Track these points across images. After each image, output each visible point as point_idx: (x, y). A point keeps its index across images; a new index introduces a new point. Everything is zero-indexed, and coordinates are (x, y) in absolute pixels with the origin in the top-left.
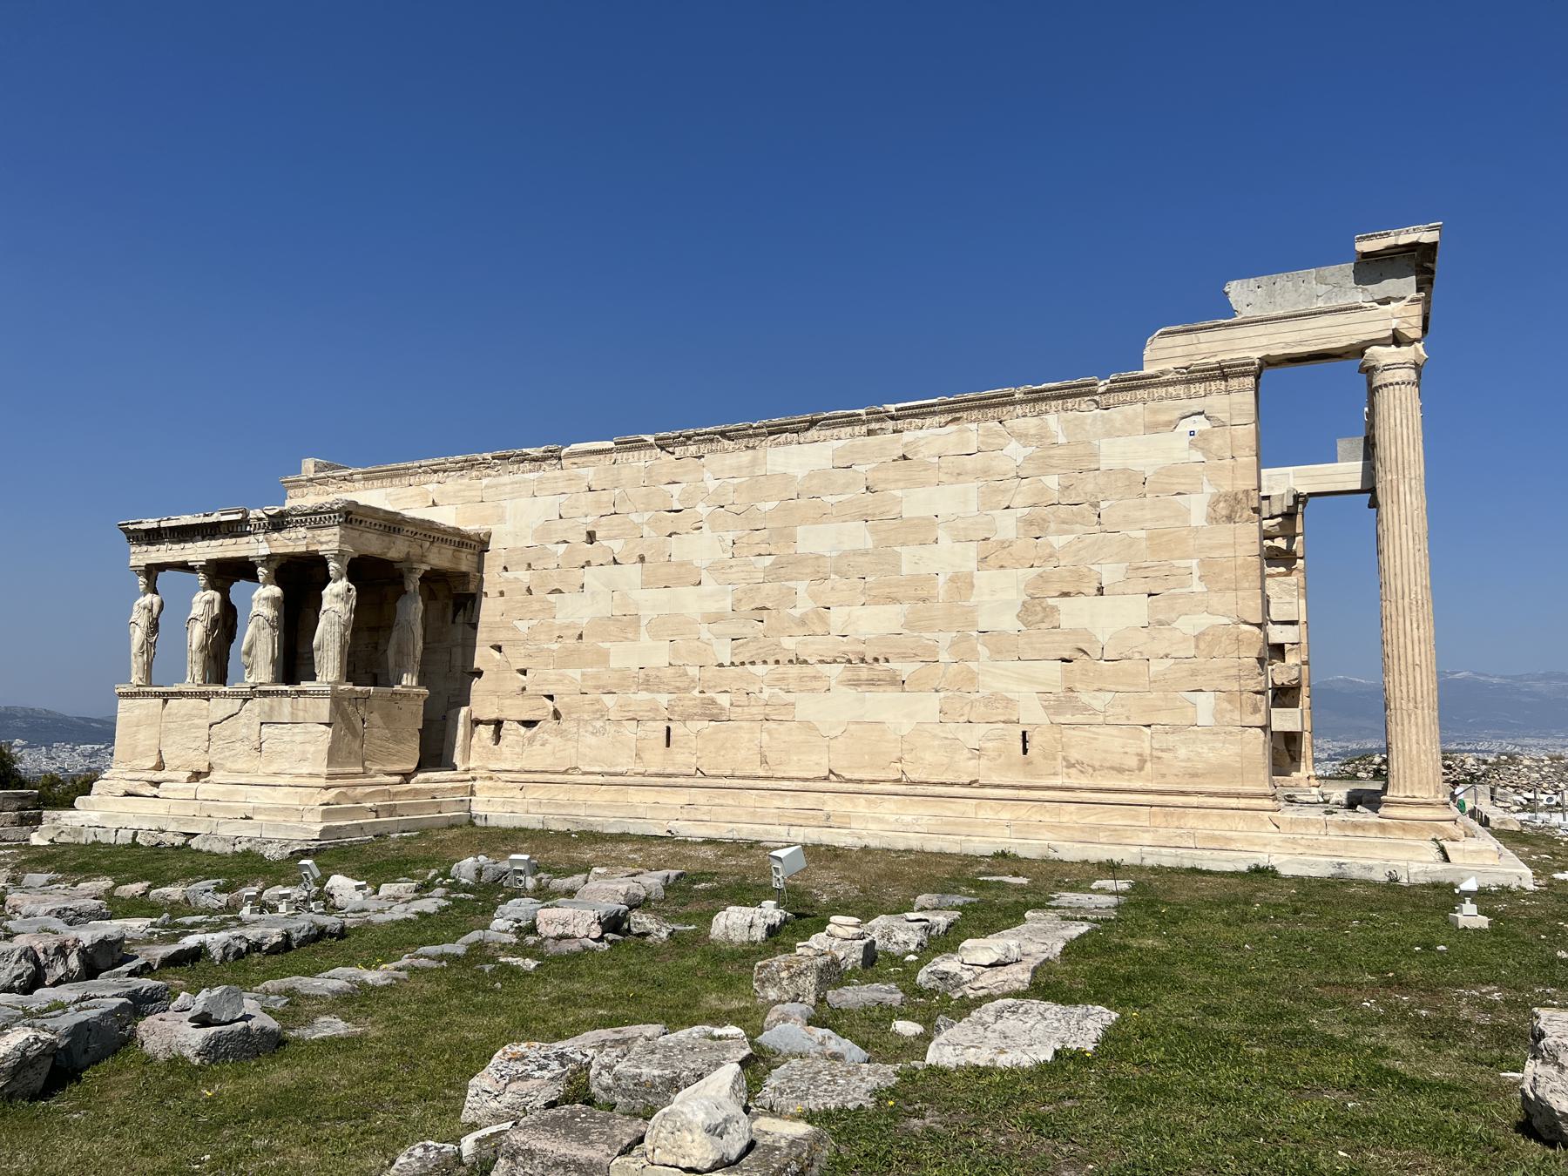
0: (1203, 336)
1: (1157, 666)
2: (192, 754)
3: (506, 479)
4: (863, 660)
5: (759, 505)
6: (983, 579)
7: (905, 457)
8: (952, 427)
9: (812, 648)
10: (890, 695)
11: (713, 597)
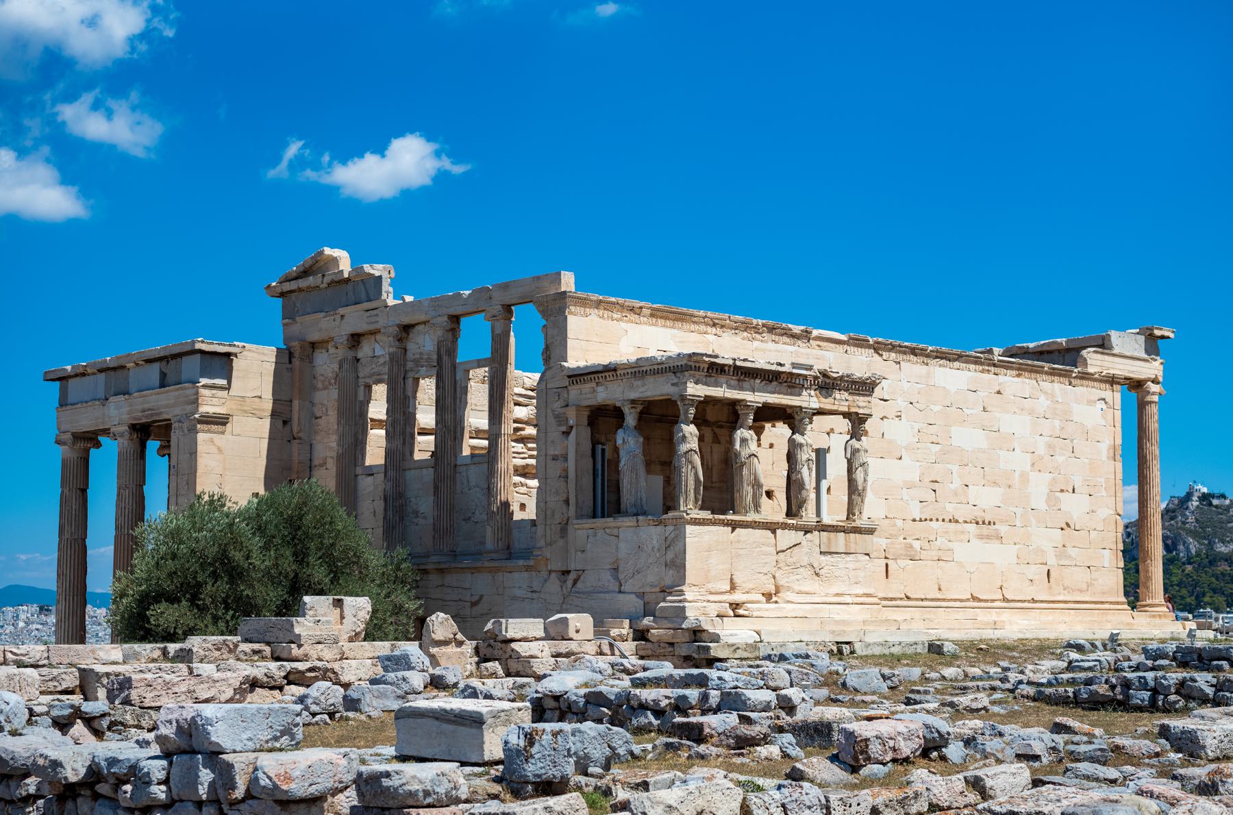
0: (1106, 357)
1: (1093, 534)
2: (763, 578)
3: (771, 345)
4: (984, 523)
5: (932, 407)
6: (1034, 476)
7: (999, 392)
8: (1016, 379)
9: (962, 513)
10: (994, 546)
11: (909, 470)
